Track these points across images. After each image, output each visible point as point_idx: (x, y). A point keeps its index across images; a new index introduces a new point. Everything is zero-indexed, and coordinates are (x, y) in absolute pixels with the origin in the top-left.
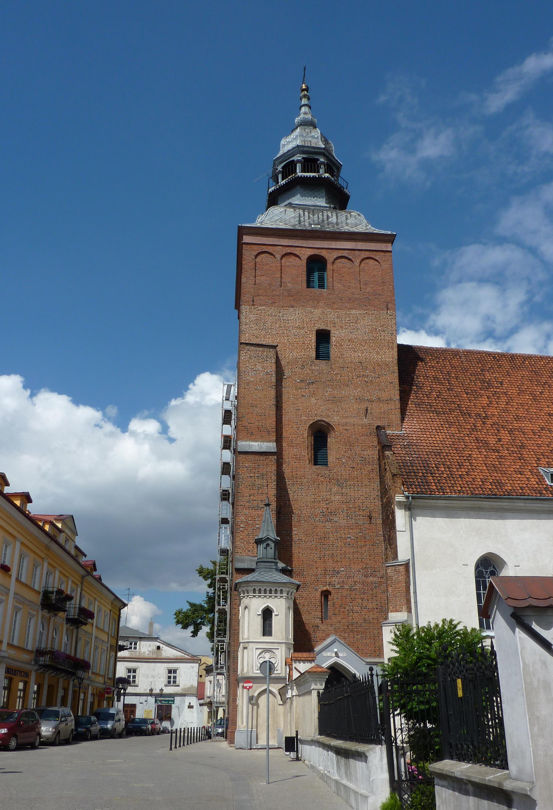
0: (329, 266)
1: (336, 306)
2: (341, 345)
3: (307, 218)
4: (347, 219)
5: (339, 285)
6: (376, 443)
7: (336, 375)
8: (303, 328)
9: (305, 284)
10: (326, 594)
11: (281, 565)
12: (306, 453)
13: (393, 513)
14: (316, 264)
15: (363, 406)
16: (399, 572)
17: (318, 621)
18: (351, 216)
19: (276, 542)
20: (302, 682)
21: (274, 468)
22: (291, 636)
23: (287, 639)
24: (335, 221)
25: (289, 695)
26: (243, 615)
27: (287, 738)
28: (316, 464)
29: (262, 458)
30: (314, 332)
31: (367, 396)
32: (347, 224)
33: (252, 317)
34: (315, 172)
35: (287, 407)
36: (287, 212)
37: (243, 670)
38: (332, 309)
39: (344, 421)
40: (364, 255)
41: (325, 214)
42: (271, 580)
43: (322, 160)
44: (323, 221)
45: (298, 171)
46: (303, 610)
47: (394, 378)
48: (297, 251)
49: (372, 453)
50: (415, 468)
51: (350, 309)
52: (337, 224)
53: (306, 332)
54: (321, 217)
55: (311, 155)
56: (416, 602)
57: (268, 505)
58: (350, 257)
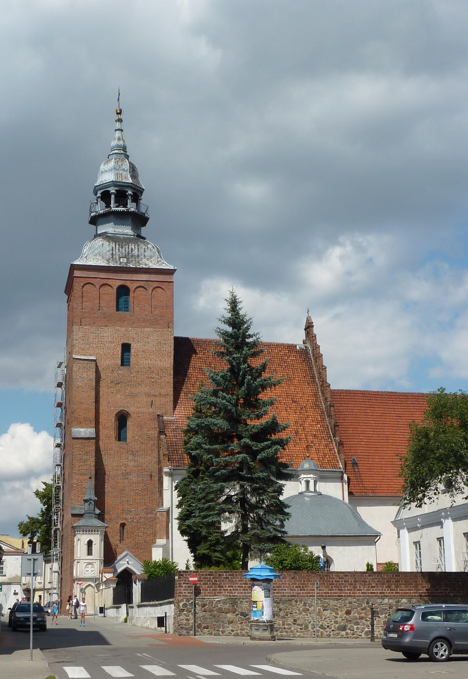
0: (131, 294)
1: (135, 325)
2: (137, 355)
3: (117, 251)
4: (145, 252)
5: (138, 309)
6: (157, 426)
7: (134, 377)
8: (114, 342)
9: (115, 308)
10: (123, 525)
11: (98, 511)
12: (113, 433)
13: (163, 478)
14: (123, 291)
15: (150, 400)
16: (163, 515)
17: (118, 542)
18: (148, 248)
19: (95, 501)
20: (107, 582)
21: (94, 447)
22: (102, 556)
23: (100, 557)
24: (136, 254)
25: (101, 588)
26: (77, 544)
27: (100, 608)
28: (119, 440)
29: (87, 441)
30: (120, 345)
31: (153, 392)
32: (145, 256)
33: (80, 335)
34: (124, 207)
35: (102, 401)
36: (104, 246)
37: (77, 574)
38: (133, 327)
39: (138, 410)
40: (156, 284)
41: (130, 247)
42: (92, 525)
43: (130, 192)
44: (128, 253)
45: (112, 206)
46: (109, 535)
47: (170, 379)
48: (110, 282)
49: (155, 433)
50: (177, 447)
51: (144, 327)
52: (138, 256)
53: (115, 346)
54: (127, 249)
55: (122, 188)
56: (172, 533)
57: (90, 478)
58: (146, 287)
